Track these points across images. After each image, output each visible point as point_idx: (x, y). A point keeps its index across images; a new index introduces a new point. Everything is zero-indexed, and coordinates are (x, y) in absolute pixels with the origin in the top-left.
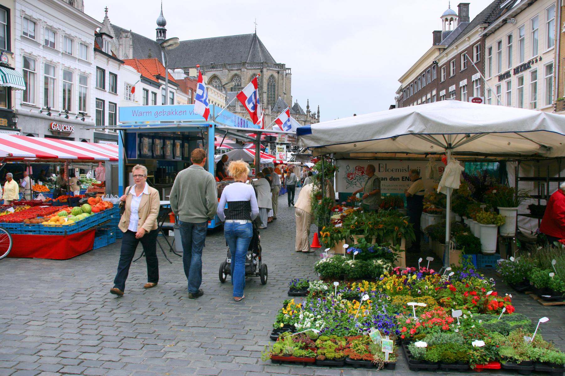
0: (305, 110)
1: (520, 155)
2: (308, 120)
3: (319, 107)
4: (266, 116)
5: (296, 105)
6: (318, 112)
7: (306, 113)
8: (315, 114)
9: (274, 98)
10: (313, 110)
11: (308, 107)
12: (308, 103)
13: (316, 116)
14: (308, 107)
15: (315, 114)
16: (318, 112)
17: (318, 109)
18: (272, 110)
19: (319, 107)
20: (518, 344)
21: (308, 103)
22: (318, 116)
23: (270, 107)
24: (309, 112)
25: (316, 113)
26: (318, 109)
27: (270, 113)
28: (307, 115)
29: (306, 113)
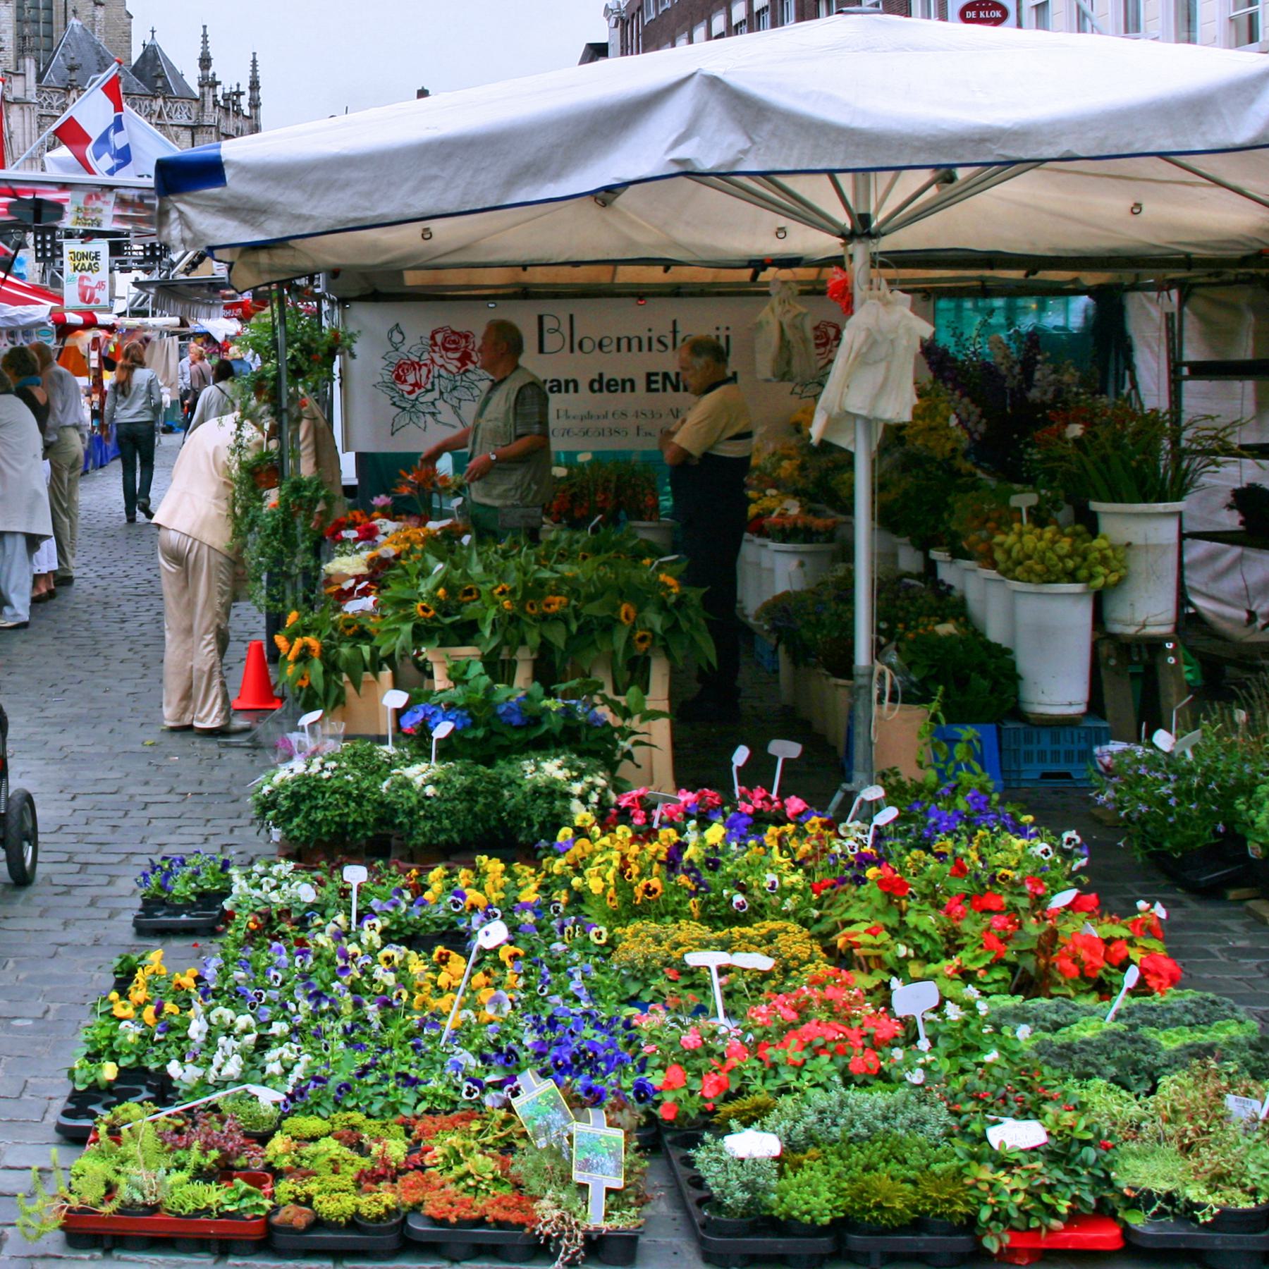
0: (192, 77)
1: (1188, 262)
2: (208, 120)
3: (254, 62)
4: (15, 108)
5: (151, 55)
6: (255, 86)
7: (197, 91)
8: (239, 94)
9: (49, 22)
10: (231, 75)
11: (205, 62)
12: (205, 42)
13: (244, 101)
14: (205, 62)
15: (239, 94)
16: (255, 86)
17: (254, 70)
18: (40, 77)
19: (254, 62)
20: (1201, 1132)
21: (205, 42)
22: (255, 104)
23: (30, 65)
24: (209, 83)
25: (245, 87)
26: (254, 70)
27: (32, 96)
28: (200, 101)
29: (197, 91)
